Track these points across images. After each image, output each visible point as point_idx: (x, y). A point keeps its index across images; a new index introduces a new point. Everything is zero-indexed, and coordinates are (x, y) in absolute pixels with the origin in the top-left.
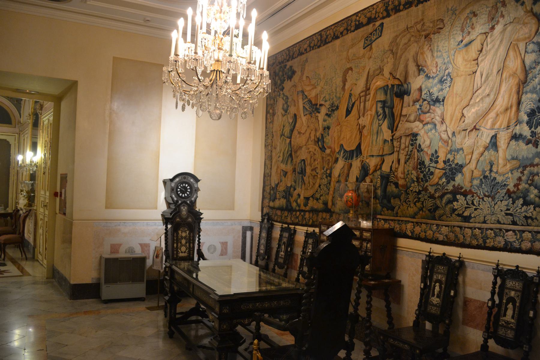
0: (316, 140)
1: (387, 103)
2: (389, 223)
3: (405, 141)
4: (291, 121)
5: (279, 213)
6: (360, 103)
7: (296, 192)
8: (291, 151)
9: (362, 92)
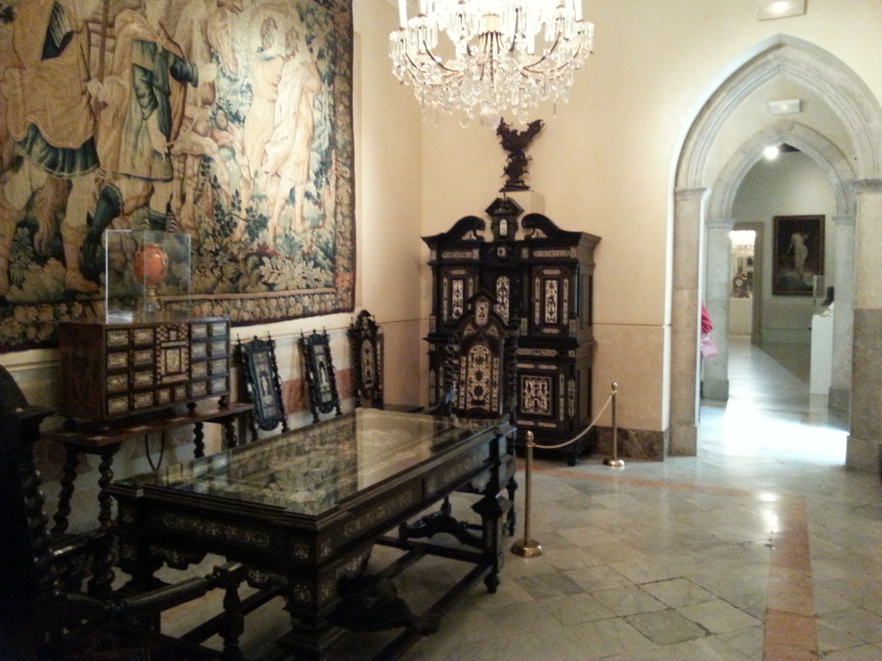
1: (157, 80)
3: (193, 166)
6: (89, 45)
9: (95, 21)
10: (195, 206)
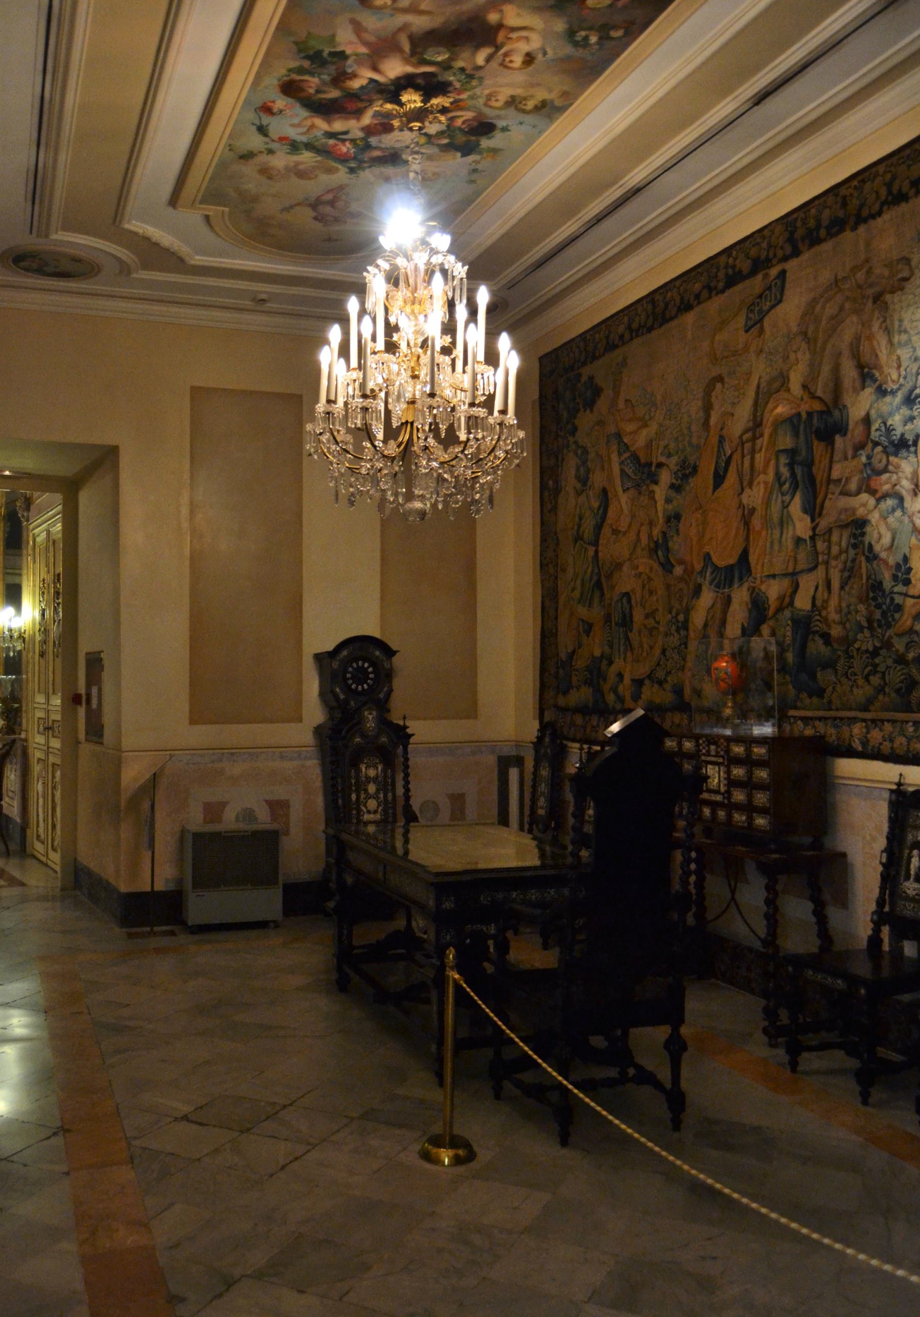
0: (652, 545)
2: (814, 727)
3: (841, 539)
4: (596, 505)
5: (579, 719)
7: (614, 669)
8: (599, 574)
10: (842, 593)
